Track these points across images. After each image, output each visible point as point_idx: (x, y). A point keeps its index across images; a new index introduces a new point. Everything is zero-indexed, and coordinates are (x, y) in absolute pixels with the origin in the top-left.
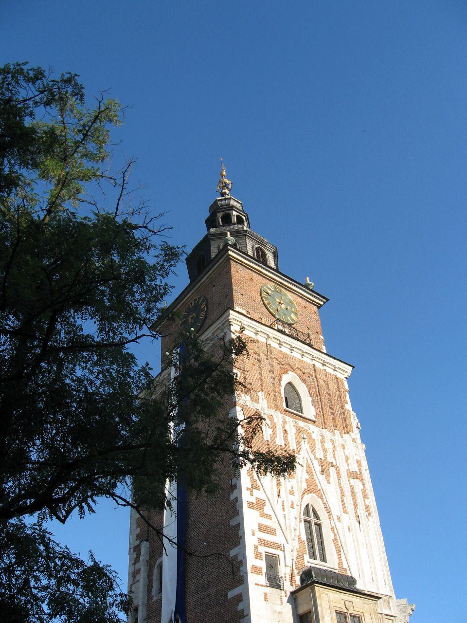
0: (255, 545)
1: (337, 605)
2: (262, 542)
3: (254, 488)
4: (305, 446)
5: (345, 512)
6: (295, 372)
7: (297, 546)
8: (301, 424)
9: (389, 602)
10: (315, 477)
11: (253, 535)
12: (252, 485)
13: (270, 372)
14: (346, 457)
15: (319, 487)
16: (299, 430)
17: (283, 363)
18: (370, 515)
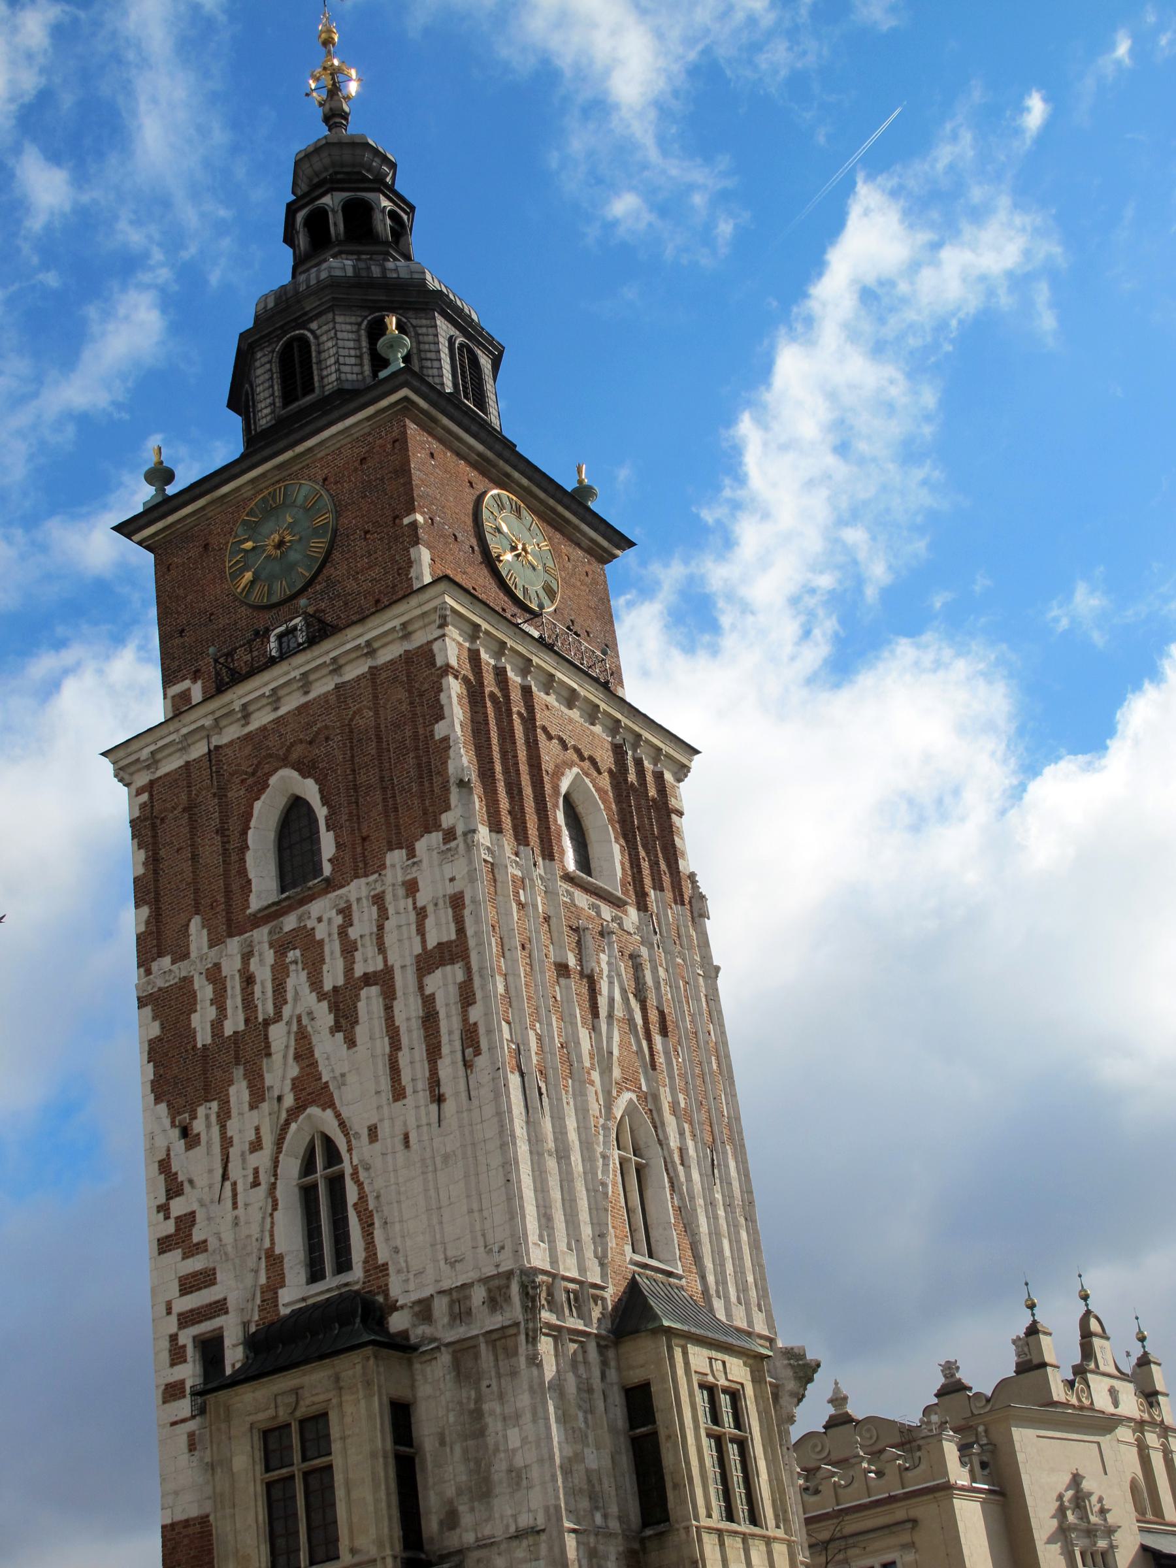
0: (171, 1336)
1: (261, 1416)
2: (186, 1319)
3: (172, 1198)
4: (297, 980)
5: (398, 1094)
6: (285, 766)
7: (263, 1280)
8: (290, 922)
9: (508, 1287)
10: (317, 1055)
11: (169, 1312)
12: (168, 1191)
13: (217, 832)
14: (421, 914)
15: (324, 1080)
16: (281, 947)
17: (250, 770)
18: (478, 1052)
